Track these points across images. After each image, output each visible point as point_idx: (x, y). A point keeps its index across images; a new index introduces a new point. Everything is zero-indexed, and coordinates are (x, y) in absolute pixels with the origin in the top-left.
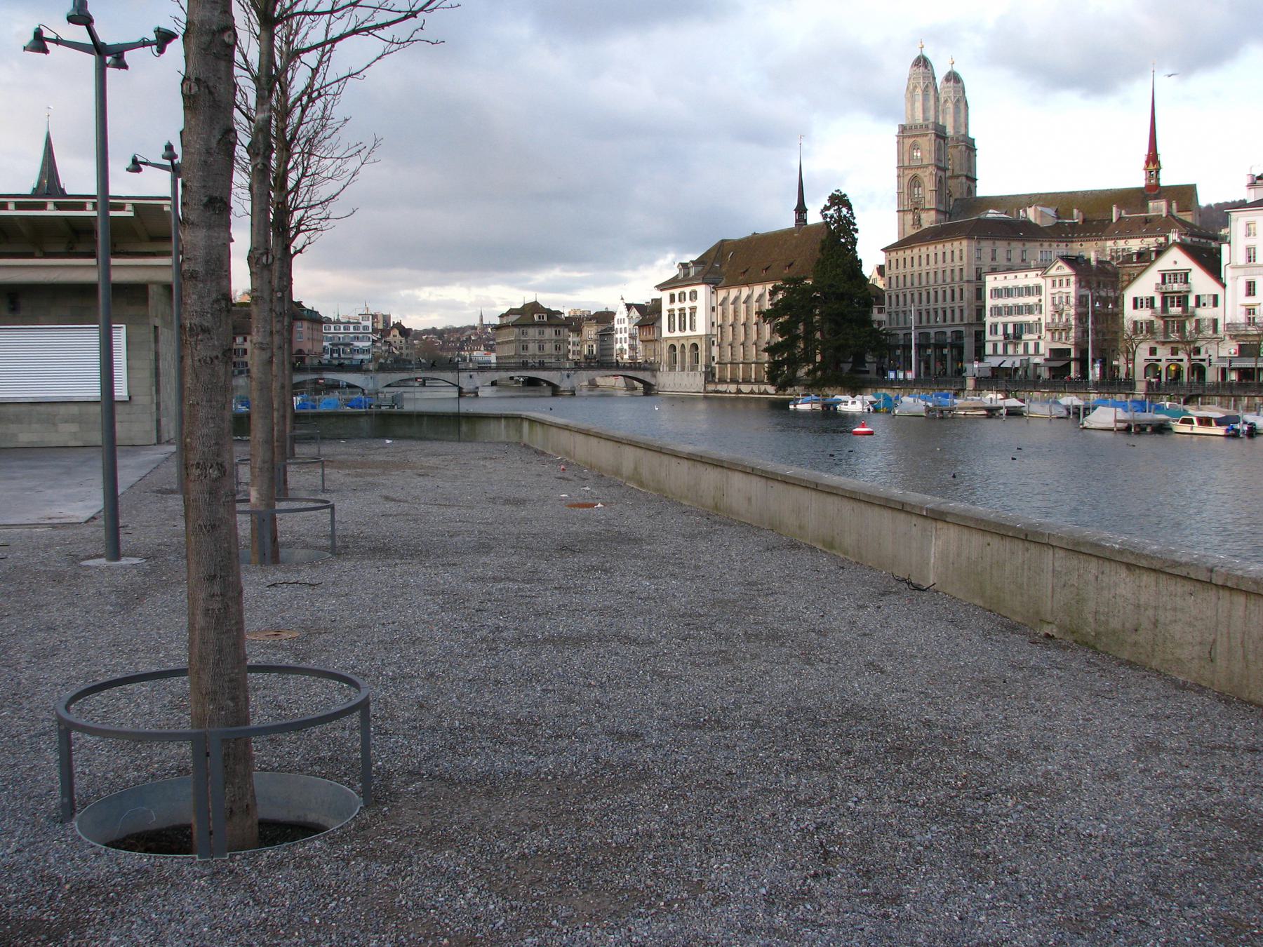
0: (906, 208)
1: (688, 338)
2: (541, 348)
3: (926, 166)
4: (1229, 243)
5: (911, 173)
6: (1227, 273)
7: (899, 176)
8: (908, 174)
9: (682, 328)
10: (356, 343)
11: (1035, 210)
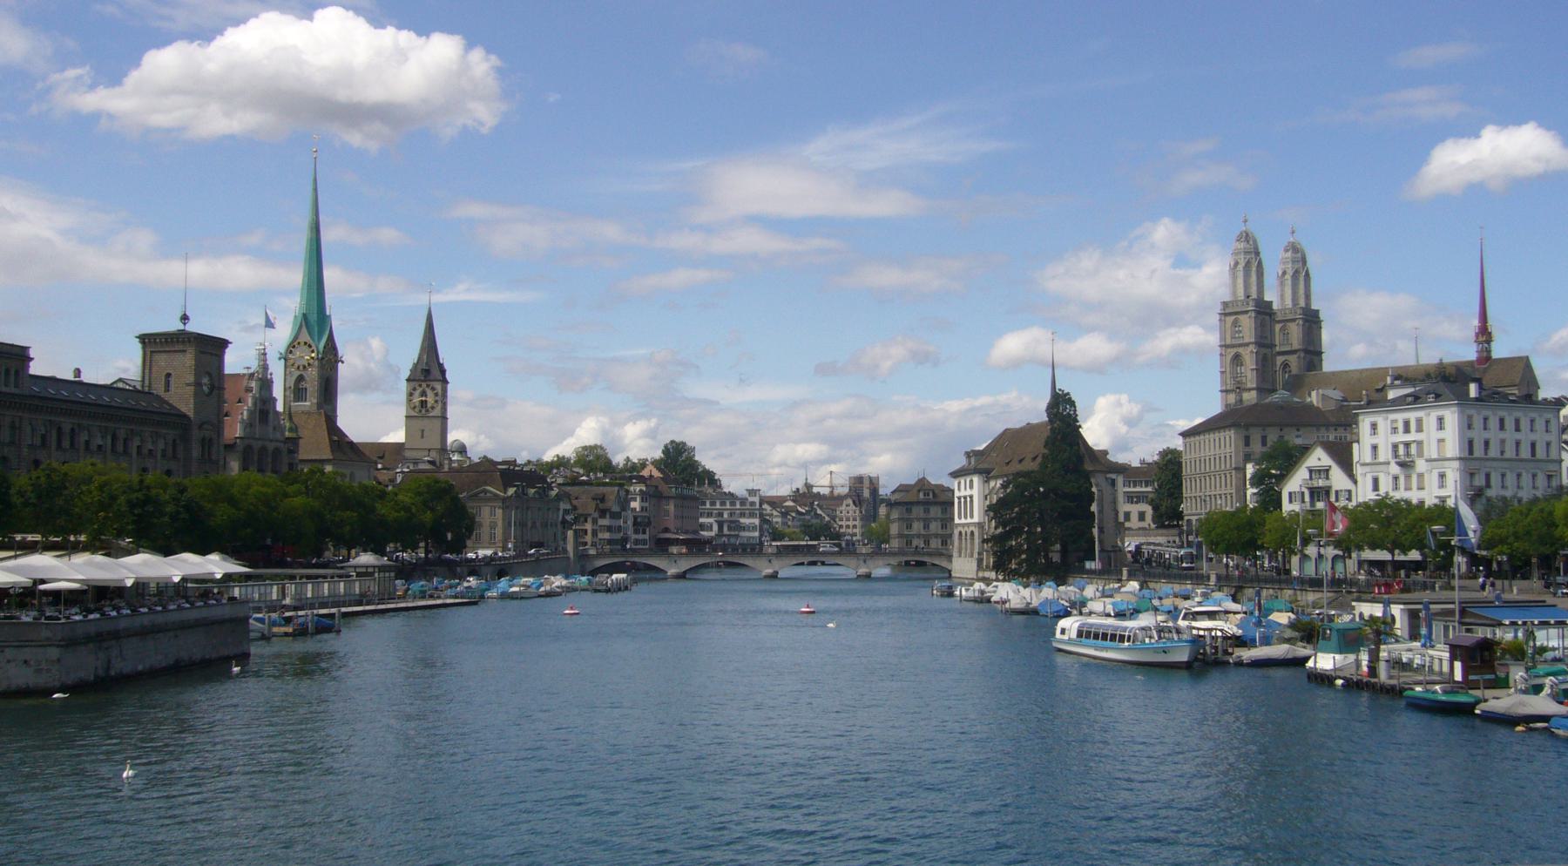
0: (1228, 388)
1: (968, 525)
2: (926, 527)
3: (1247, 345)
4: (1358, 442)
5: (1232, 352)
6: (1358, 471)
7: (1221, 355)
8: (1230, 353)
9: (966, 518)
10: (742, 520)
11: (1318, 394)
